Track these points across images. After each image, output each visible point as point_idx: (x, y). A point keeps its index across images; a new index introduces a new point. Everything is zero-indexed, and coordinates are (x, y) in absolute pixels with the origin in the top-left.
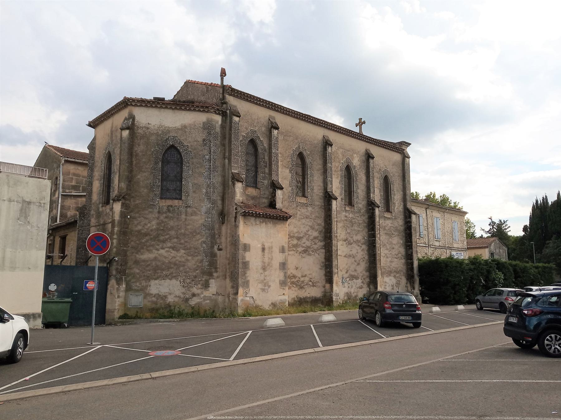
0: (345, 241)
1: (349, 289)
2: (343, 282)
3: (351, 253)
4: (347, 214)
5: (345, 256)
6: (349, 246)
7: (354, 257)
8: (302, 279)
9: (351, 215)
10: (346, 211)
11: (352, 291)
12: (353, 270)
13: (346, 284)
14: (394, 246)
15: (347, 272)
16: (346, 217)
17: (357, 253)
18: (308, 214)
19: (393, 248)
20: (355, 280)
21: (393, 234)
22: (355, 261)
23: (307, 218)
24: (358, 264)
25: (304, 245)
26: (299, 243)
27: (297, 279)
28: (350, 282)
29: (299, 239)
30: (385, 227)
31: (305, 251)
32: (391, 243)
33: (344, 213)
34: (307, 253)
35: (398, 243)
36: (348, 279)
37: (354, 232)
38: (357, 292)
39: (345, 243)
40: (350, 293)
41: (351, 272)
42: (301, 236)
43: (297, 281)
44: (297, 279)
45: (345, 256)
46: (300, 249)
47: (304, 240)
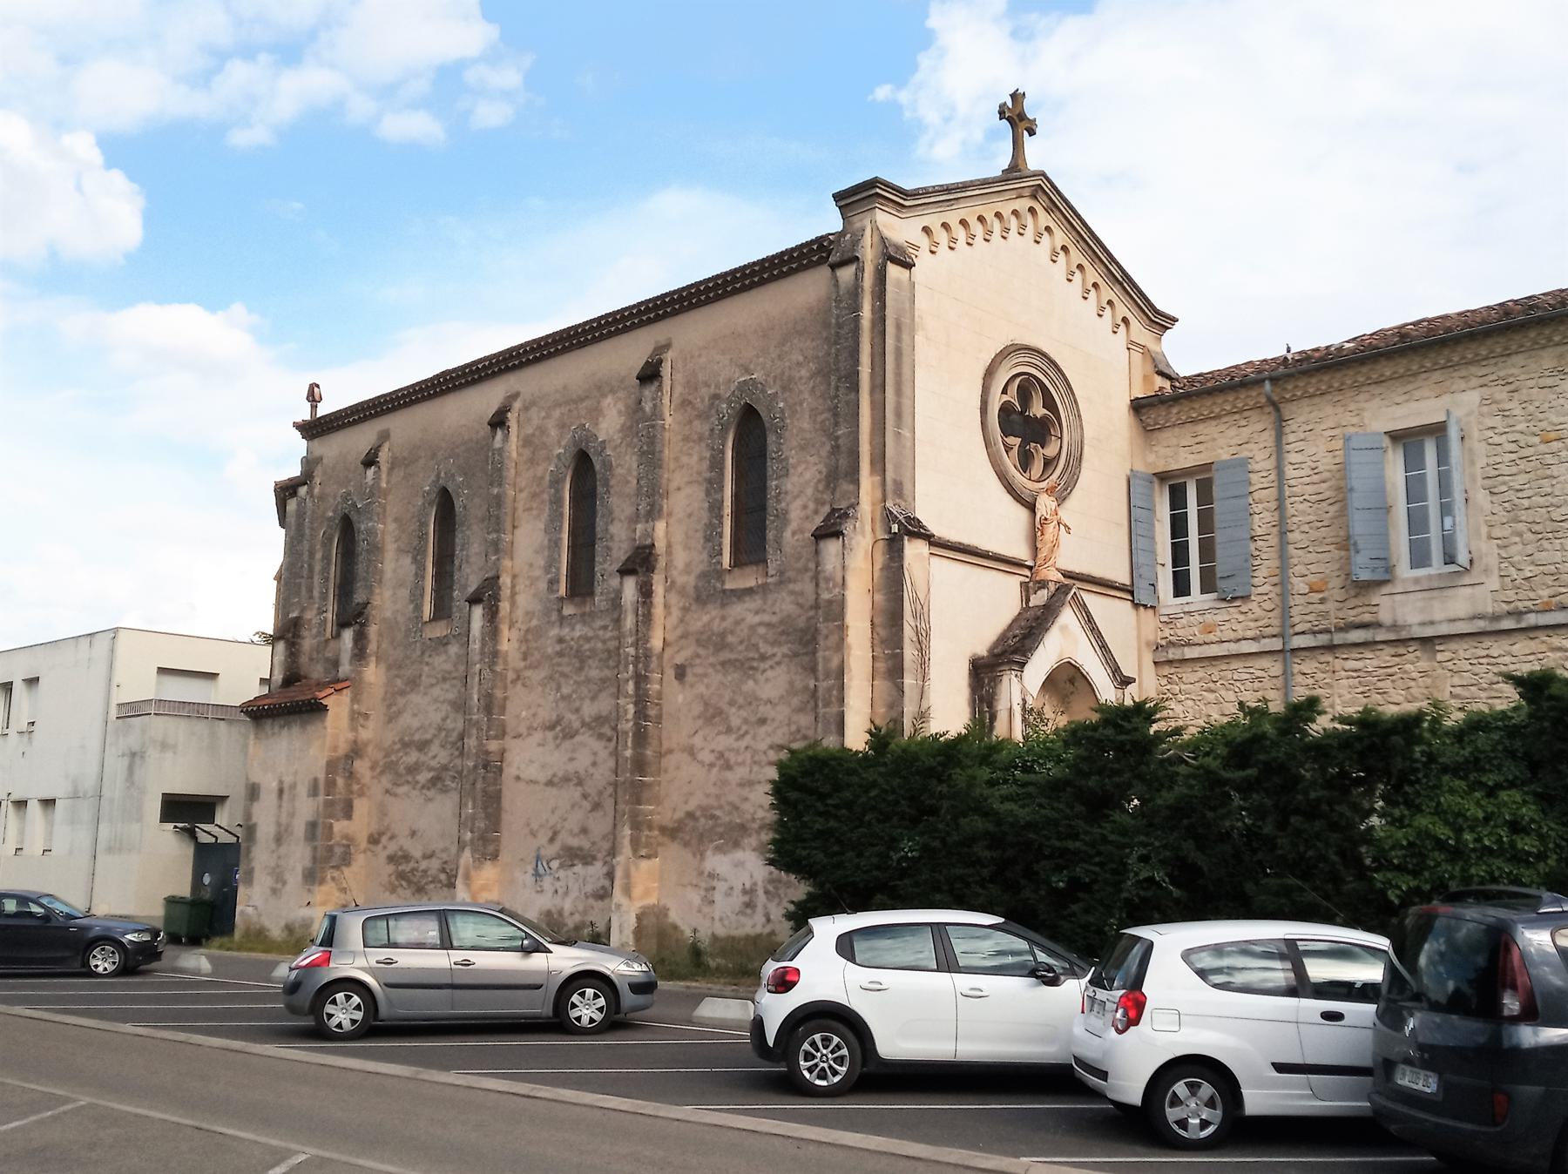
0: (552, 727)
1: (558, 900)
2: (537, 874)
3: (571, 768)
4: (566, 631)
5: (550, 783)
6: (567, 744)
7: (580, 783)
8: (424, 865)
9: (580, 630)
10: (562, 619)
11: (568, 906)
12: (576, 830)
13: (547, 882)
14: (764, 710)
15: (552, 840)
16: (561, 640)
17: (594, 764)
18: (448, 667)
19: (763, 721)
20: (579, 868)
21: (763, 658)
22: (585, 796)
23: (444, 679)
24: (596, 806)
25: (433, 763)
26: (423, 758)
27: (412, 864)
28: (561, 874)
29: (423, 746)
30: (723, 635)
31: (434, 781)
32: (752, 700)
33: (554, 632)
34: (439, 785)
35: (792, 690)
36: (555, 864)
37: (584, 690)
38: (585, 912)
39: (550, 735)
40: (560, 913)
41: (566, 839)
42: (428, 736)
43: (413, 870)
44: (412, 864)
45: (550, 783)
46: (424, 777)
47: (435, 748)
